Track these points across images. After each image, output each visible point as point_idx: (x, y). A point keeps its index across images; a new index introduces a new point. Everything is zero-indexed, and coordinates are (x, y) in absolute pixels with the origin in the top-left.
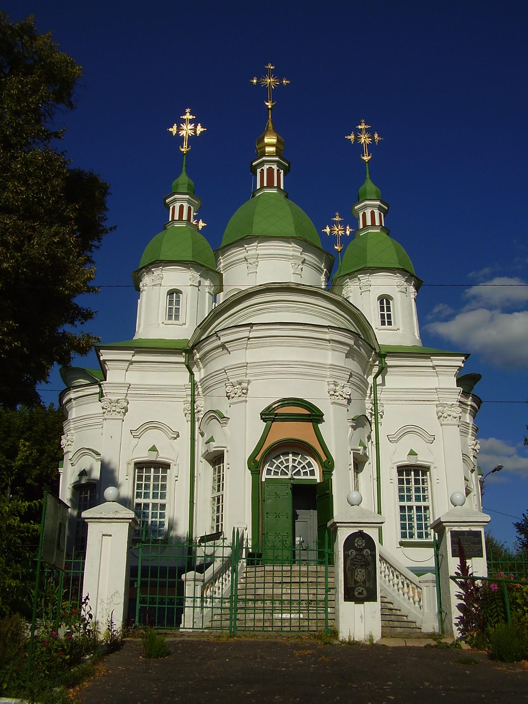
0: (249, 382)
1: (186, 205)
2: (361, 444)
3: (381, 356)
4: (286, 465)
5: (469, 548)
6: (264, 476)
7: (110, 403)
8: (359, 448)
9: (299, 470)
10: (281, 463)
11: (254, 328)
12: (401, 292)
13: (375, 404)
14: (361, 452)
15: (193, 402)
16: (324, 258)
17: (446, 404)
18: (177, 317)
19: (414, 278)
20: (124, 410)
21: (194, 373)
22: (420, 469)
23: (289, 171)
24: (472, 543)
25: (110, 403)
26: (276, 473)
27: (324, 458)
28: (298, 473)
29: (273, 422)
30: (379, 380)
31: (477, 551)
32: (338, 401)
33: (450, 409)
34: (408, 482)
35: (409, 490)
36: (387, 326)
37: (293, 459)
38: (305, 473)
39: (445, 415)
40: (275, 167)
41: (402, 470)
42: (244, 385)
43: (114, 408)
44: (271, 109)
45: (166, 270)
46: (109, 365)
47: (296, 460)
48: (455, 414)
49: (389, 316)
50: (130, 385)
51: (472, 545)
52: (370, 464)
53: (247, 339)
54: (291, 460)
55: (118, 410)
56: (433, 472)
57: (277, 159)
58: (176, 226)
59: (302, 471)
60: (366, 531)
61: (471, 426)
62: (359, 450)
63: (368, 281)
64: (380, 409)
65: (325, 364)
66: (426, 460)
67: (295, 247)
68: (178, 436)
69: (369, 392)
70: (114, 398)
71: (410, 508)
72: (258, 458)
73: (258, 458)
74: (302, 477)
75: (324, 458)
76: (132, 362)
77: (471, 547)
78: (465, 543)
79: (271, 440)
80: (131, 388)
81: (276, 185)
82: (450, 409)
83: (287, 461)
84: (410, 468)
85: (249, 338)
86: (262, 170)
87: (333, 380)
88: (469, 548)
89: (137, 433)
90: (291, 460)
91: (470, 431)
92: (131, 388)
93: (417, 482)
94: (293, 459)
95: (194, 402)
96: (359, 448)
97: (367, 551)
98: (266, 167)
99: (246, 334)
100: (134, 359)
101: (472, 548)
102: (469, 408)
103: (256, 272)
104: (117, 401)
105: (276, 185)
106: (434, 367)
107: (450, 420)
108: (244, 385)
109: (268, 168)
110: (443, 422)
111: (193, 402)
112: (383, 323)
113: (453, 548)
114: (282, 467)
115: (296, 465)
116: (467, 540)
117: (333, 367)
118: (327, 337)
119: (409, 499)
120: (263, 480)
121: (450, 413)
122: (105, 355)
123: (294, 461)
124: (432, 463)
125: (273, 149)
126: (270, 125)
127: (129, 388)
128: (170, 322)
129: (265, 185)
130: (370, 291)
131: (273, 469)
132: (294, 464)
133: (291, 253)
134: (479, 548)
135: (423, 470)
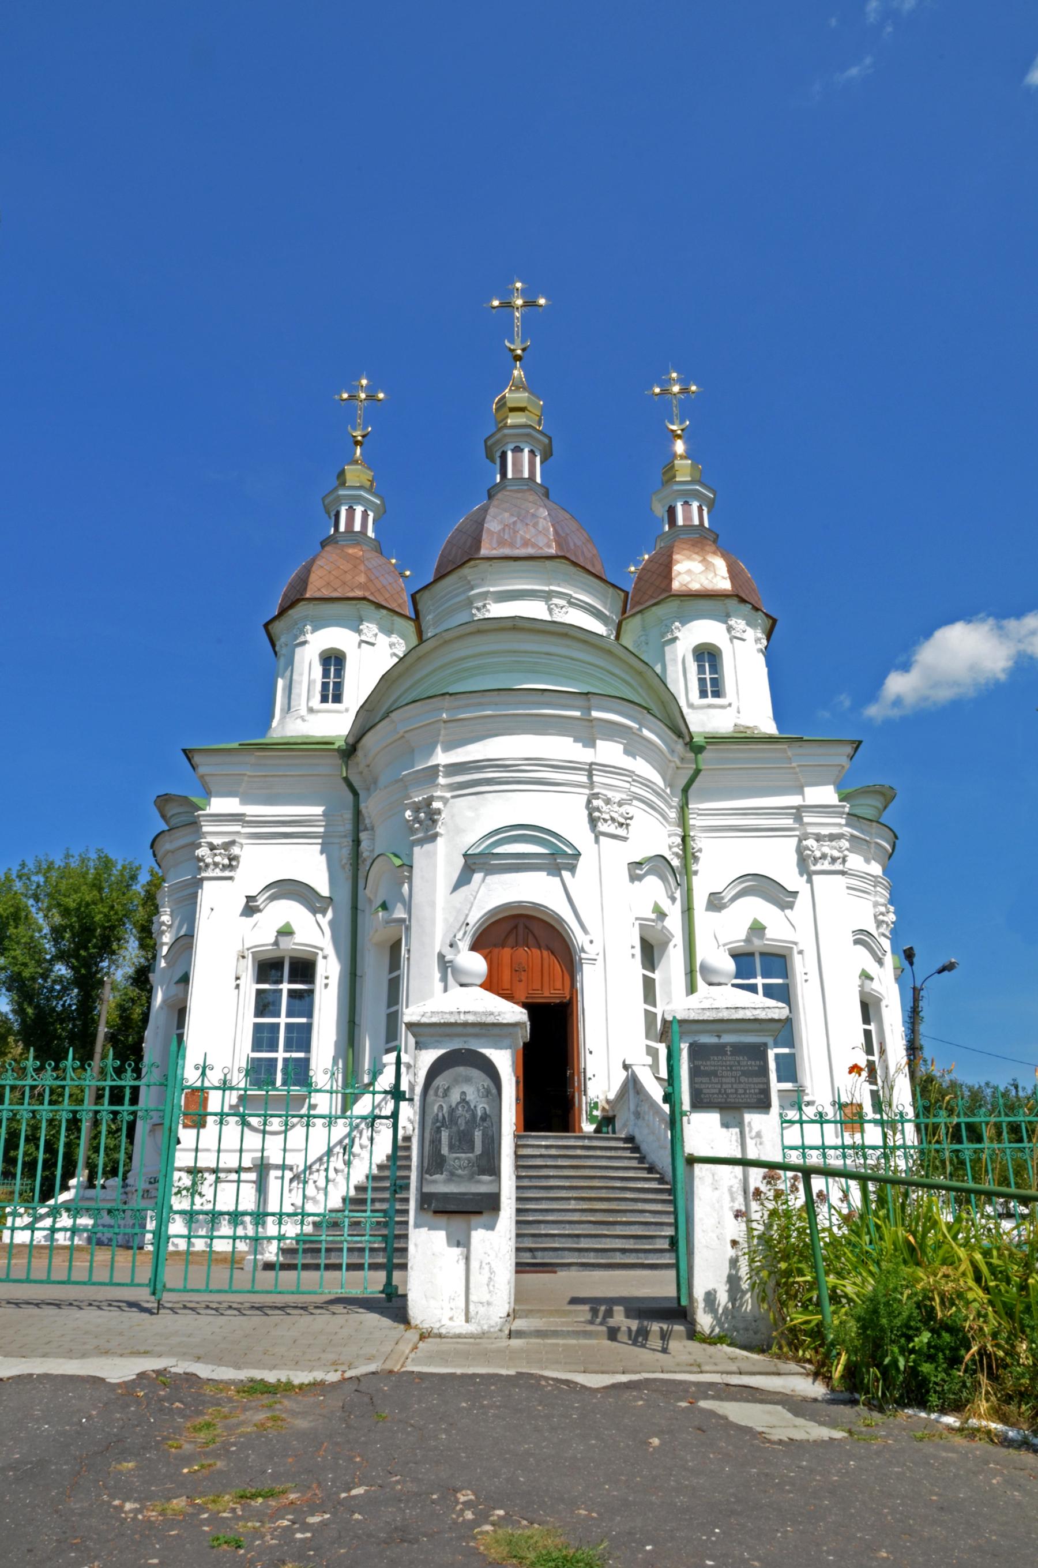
5: (735, 1086)
15: (357, 842)
16: (610, 595)
18: (338, 698)
20: (234, 863)
21: (359, 792)
24: (744, 1073)
25: (211, 850)
31: (756, 1094)
36: (710, 700)
39: (818, 854)
42: (436, 805)
43: (218, 859)
48: (836, 854)
49: (715, 682)
51: (743, 1079)
52: (675, 946)
55: (226, 861)
56: (797, 959)
70: (217, 841)
77: (740, 1083)
78: (725, 1073)
88: (735, 1086)
101: (742, 1086)
104: (227, 846)
107: (826, 865)
108: (436, 805)
113: (697, 1086)
116: (731, 1066)
121: (826, 850)
124: (796, 944)
128: (325, 706)
134: (761, 1086)
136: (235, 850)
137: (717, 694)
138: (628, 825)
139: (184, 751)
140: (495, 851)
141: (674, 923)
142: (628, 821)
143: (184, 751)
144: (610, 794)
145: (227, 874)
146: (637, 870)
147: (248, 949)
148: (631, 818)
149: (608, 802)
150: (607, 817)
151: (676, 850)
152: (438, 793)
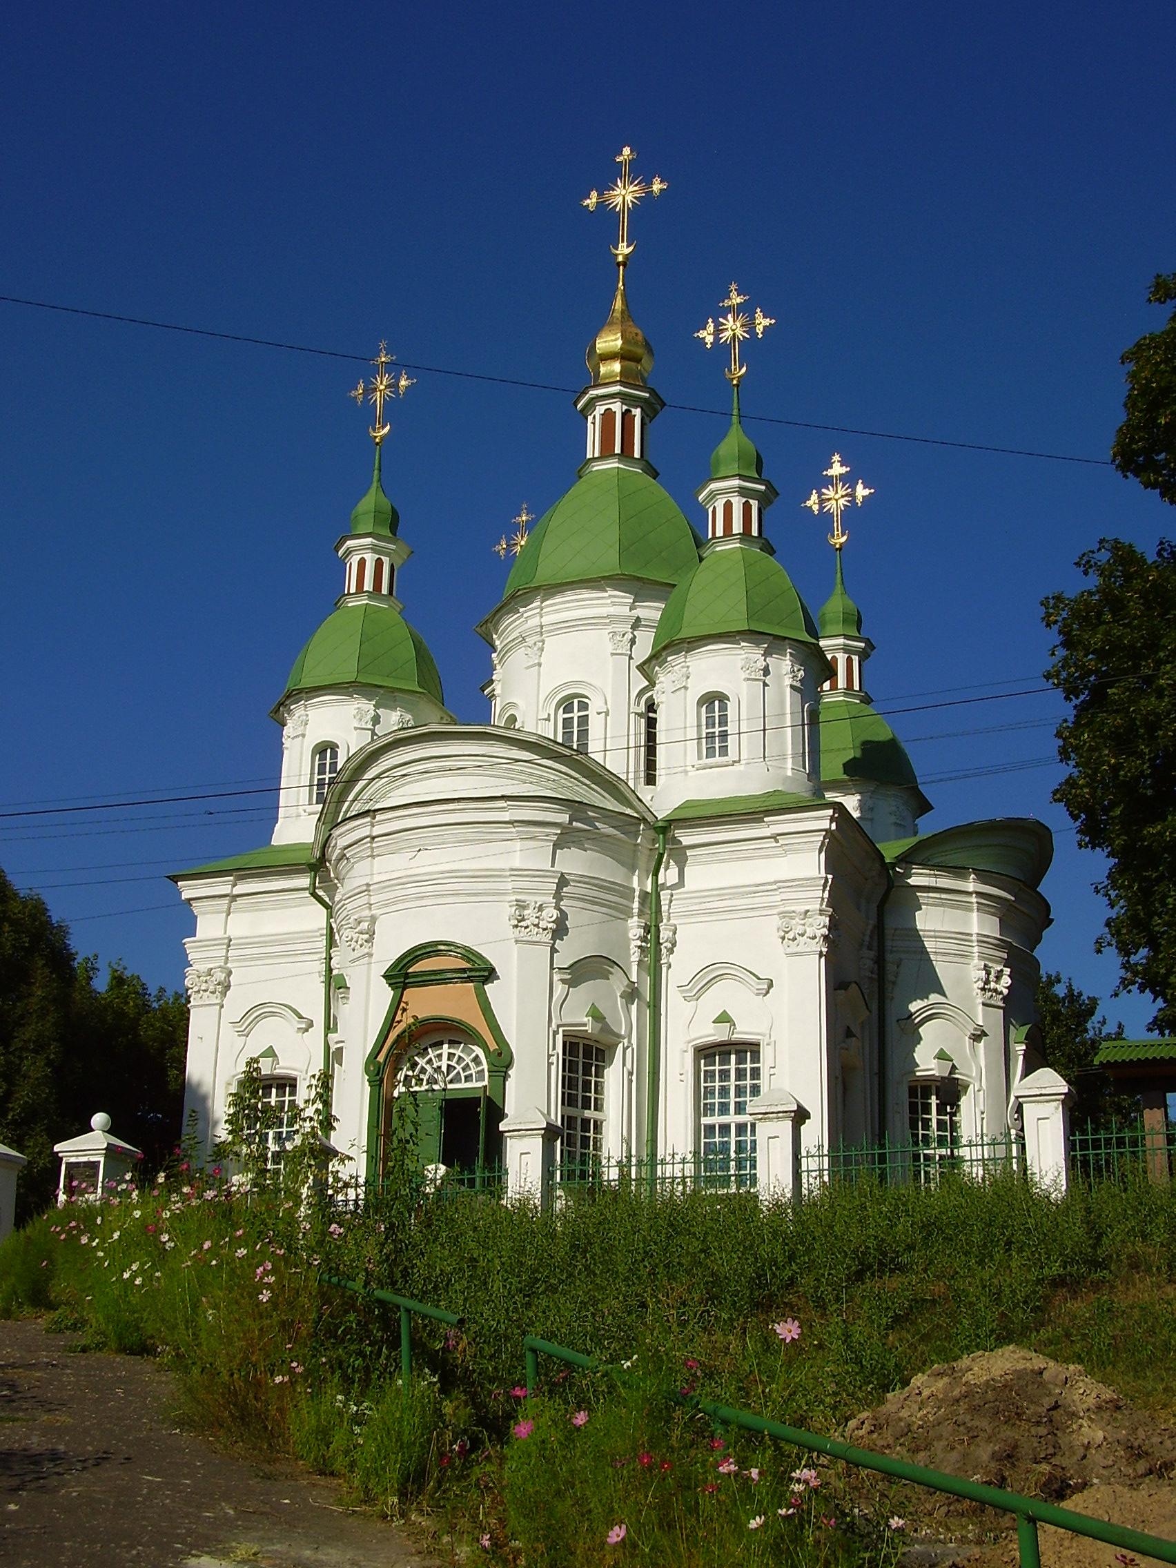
0: (373, 919)
1: (370, 558)
3: (665, 828)
7: (199, 977)
8: (586, 1020)
9: (459, 1073)
10: (430, 1062)
11: (378, 818)
12: (748, 679)
13: (652, 930)
14: (589, 1028)
17: (794, 912)
19: (787, 641)
22: (733, 1048)
27: (493, 1046)
28: (457, 1079)
29: (404, 989)
30: (669, 875)
33: (803, 922)
34: (725, 1075)
35: (724, 1091)
36: (717, 759)
37: (449, 1054)
38: (468, 1078)
40: (617, 407)
41: (706, 1053)
44: (624, 264)
45: (314, 705)
46: (197, 907)
47: (454, 1055)
50: (230, 940)
53: (368, 839)
54: (445, 1057)
56: (766, 1053)
57: (617, 388)
58: (350, 605)
59: (463, 1075)
61: (974, 938)
62: (585, 1025)
63: (683, 667)
65: (503, 870)
66: (752, 1030)
67: (615, 596)
68: (771, 985)
71: (725, 1129)
72: (381, 1058)
73: (381, 1058)
75: (493, 1046)
76: (234, 898)
79: (405, 1021)
80: (234, 945)
82: (803, 922)
83: (439, 1056)
85: (373, 838)
86: (594, 417)
87: (514, 898)
89: (241, 1026)
90: (445, 1057)
91: (976, 949)
92: (234, 945)
93: (740, 1074)
94: (449, 1054)
95: (331, 958)
96: (586, 1020)
99: (366, 831)
100: (237, 891)
102: (974, 899)
103: (540, 665)
105: (618, 450)
106: (775, 837)
109: (602, 412)
110: (789, 950)
112: (710, 753)
115: (453, 1063)
117: (517, 873)
118: (506, 816)
119: (724, 1109)
122: (189, 890)
123: (450, 1056)
125: (616, 367)
126: (618, 304)
127: (229, 946)
129: (597, 455)
130: (686, 688)
132: (450, 1063)
133: (603, 611)
135: (749, 1050)
147: (234, 1076)
151: (639, 943)
152: (367, 913)
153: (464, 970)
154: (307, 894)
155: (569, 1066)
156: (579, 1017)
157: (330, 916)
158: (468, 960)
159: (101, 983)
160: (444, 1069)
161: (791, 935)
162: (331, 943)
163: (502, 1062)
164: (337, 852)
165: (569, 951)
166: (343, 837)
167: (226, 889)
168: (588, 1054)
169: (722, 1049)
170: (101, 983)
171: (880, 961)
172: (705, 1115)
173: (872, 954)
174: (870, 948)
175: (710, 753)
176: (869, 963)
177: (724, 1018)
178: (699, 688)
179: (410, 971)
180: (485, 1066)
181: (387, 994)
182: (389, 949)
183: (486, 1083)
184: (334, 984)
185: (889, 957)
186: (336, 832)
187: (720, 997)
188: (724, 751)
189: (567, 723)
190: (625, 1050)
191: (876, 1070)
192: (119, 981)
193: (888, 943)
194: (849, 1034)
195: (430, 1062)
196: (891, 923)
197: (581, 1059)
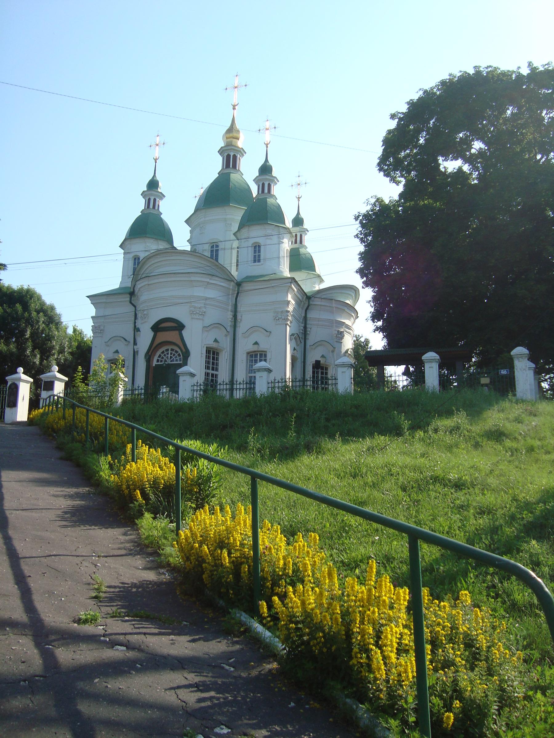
2: (216, 341)
3: (239, 284)
4: (167, 356)
6: (155, 363)
13: (235, 316)
15: (135, 323)
20: (102, 331)
23: (246, 153)
26: (161, 361)
27: (184, 350)
32: (196, 317)
36: (257, 263)
38: (177, 360)
48: (283, 318)
52: (225, 352)
54: (169, 354)
59: (175, 359)
60: (16, 382)
64: (239, 317)
69: (230, 308)
72: (150, 354)
73: (150, 354)
74: (175, 362)
75: (184, 350)
79: (157, 342)
81: (231, 166)
83: (168, 354)
84: (257, 353)
85: (149, 285)
90: (169, 354)
97: (15, 390)
98: (225, 155)
99: (147, 283)
105: (231, 166)
111: (135, 323)
112: (255, 261)
114: (165, 358)
115: (172, 356)
120: (154, 365)
121: (280, 317)
123: (171, 354)
131: (160, 359)
136: (102, 328)
137: (259, 261)
138: (204, 315)
139: (87, 297)
140: (160, 326)
141: (225, 344)
142: (204, 314)
143: (87, 297)
144: (196, 305)
145: (100, 335)
146: (206, 328)
148: (205, 312)
149: (195, 307)
150: (195, 313)
151: (230, 320)
153: (176, 327)
154: (129, 303)
155: (208, 357)
156: (210, 343)
157: (136, 310)
158: (177, 324)
159: (70, 331)
160: (169, 357)
161: (277, 318)
162: (136, 318)
163: (186, 354)
164: (138, 289)
165: (208, 322)
166: (139, 285)
167: (104, 301)
168: (214, 353)
169: (255, 353)
170: (70, 331)
171: (305, 327)
172: (249, 373)
173: (303, 325)
174: (302, 323)
175: (255, 261)
176: (302, 328)
177: (256, 343)
178: (251, 242)
179: (160, 326)
180: (182, 357)
181: (151, 334)
182: (153, 321)
183: (181, 362)
184: (136, 330)
185: (308, 326)
186: (137, 283)
187: (255, 337)
188: (259, 261)
189: (212, 251)
190: (225, 352)
191: (303, 361)
192: (75, 330)
193: (308, 322)
194: (294, 349)
195: (165, 355)
196: (309, 316)
197: (211, 355)
